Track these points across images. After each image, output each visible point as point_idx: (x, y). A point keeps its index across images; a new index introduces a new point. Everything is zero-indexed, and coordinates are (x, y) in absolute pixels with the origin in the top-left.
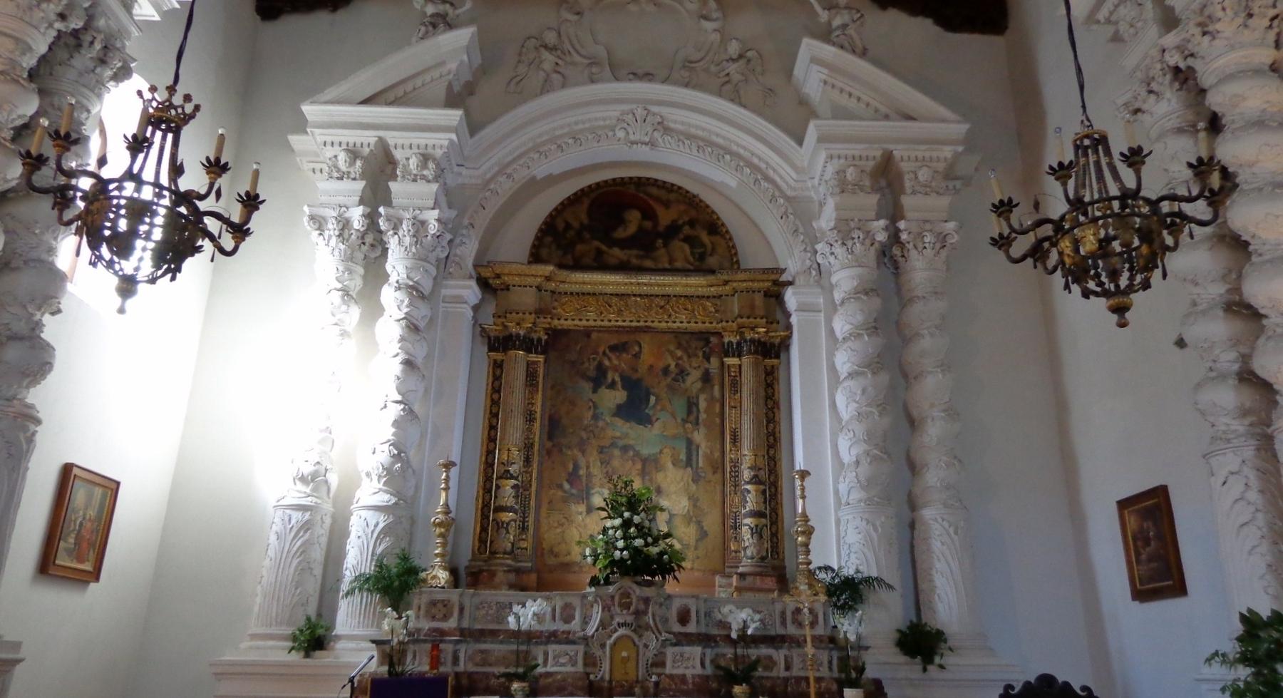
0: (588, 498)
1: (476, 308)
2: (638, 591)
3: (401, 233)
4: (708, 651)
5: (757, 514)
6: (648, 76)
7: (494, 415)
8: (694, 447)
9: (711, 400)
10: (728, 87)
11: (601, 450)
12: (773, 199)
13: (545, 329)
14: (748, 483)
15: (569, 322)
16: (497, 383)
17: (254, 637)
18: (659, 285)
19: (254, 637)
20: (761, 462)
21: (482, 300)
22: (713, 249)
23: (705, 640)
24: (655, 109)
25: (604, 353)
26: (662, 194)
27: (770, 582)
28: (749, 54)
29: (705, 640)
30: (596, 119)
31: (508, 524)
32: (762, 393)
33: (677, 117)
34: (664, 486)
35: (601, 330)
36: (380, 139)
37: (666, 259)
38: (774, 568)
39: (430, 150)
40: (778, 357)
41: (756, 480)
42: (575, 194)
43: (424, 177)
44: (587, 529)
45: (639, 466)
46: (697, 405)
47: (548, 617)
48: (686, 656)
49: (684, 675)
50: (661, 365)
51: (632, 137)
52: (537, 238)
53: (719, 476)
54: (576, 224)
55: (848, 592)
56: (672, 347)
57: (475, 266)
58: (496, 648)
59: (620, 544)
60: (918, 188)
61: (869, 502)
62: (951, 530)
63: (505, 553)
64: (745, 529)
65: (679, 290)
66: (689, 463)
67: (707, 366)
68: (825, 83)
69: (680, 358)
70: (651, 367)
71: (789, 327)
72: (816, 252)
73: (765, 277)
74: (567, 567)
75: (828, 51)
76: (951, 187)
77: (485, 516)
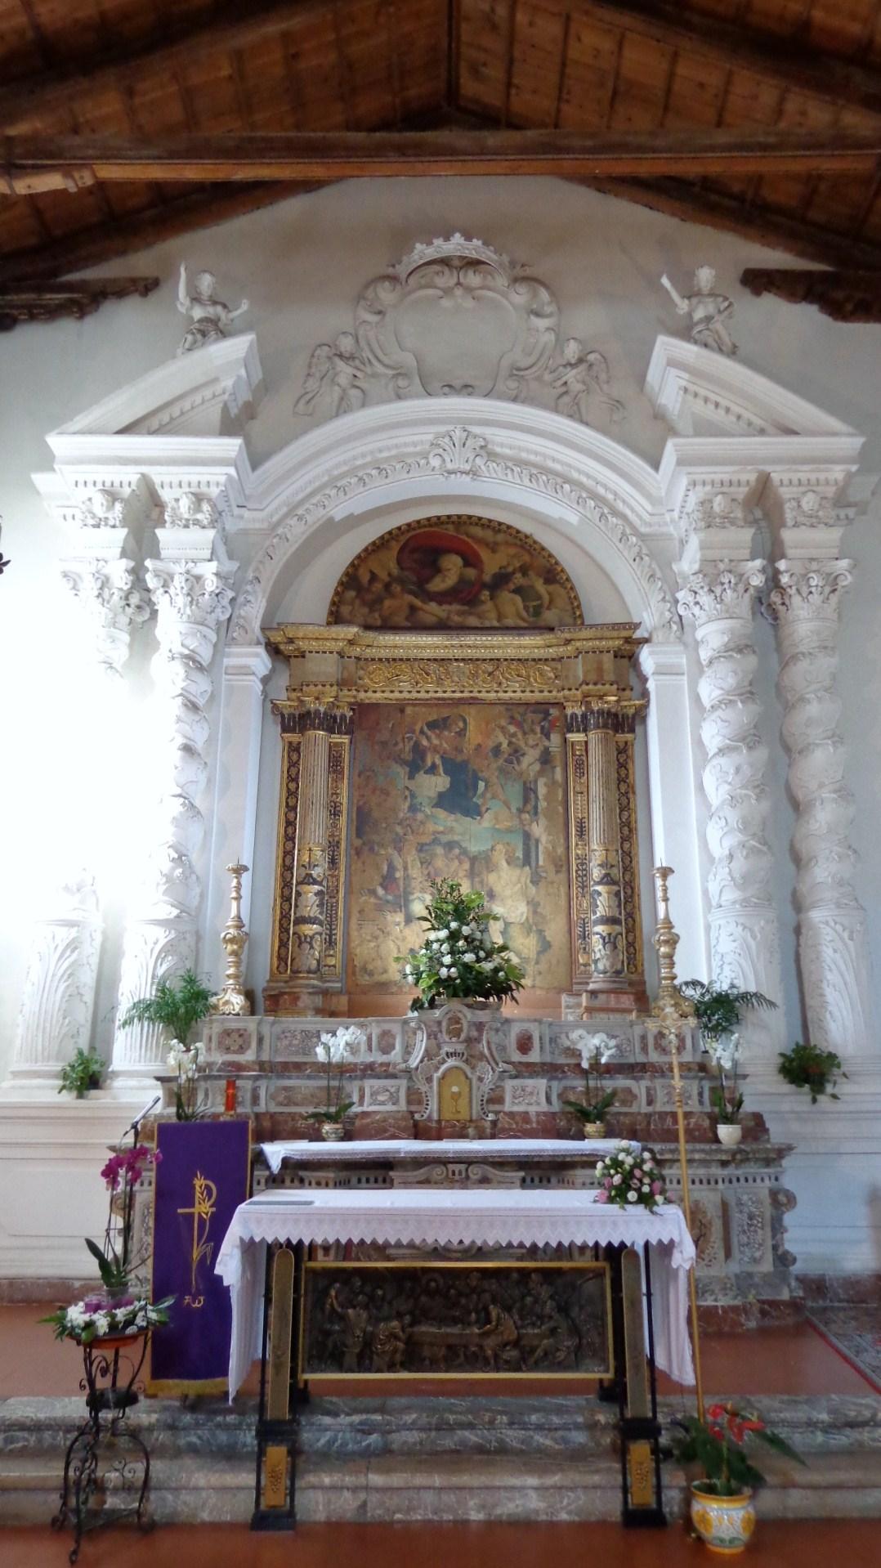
0: (406, 906)
1: (265, 681)
2: (468, 1016)
3: (172, 591)
4: (555, 1084)
5: (611, 921)
6: (467, 389)
7: (291, 808)
8: (532, 842)
9: (552, 784)
10: (566, 399)
11: (421, 848)
12: (623, 538)
13: (350, 704)
14: (599, 883)
15: (379, 695)
16: (293, 771)
17: (16, 1074)
18: (486, 647)
19: (16, 1074)
20: (614, 858)
21: (273, 670)
22: (551, 602)
23: (550, 1070)
24: (476, 430)
25: (422, 732)
26: (488, 535)
27: (627, 1001)
28: (591, 357)
29: (550, 1070)
30: (406, 445)
31: (312, 938)
33: (501, 439)
34: (497, 889)
35: (416, 703)
36: (143, 475)
37: (493, 615)
38: (631, 984)
39: (204, 489)
40: (632, 730)
41: (608, 880)
42: (382, 537)
43: (197, 522)
44: (405, 943)
45: (467, 866)
46: (535, 792)
47: (363, 1047)
48: (529, 1090)
49: (527, 1113)
50: (491, 744)
51: (450, 466)
52: (337, 593)
53: (563, 876)
54: (383, 575)
55: (721, 1010)
56: (503, 722)
57: (263, 629)
58: (304, 1085)
59: (447, 960)
60: (801, 519)
61: (745, 903)
62: (846, 935)
63: (309, 972)
64: (595, 938)
65: (511, 653)
66: (527, 861)
67: (547, 743)
68: (686, 390)
69: (514, 735)
70: (479, 745)
71: (645, 694)
72: (677, 601)
73: (615, 634)
74: (384, 987)
75: (688, 351)
76: (842, 516)
77: (284, 930)
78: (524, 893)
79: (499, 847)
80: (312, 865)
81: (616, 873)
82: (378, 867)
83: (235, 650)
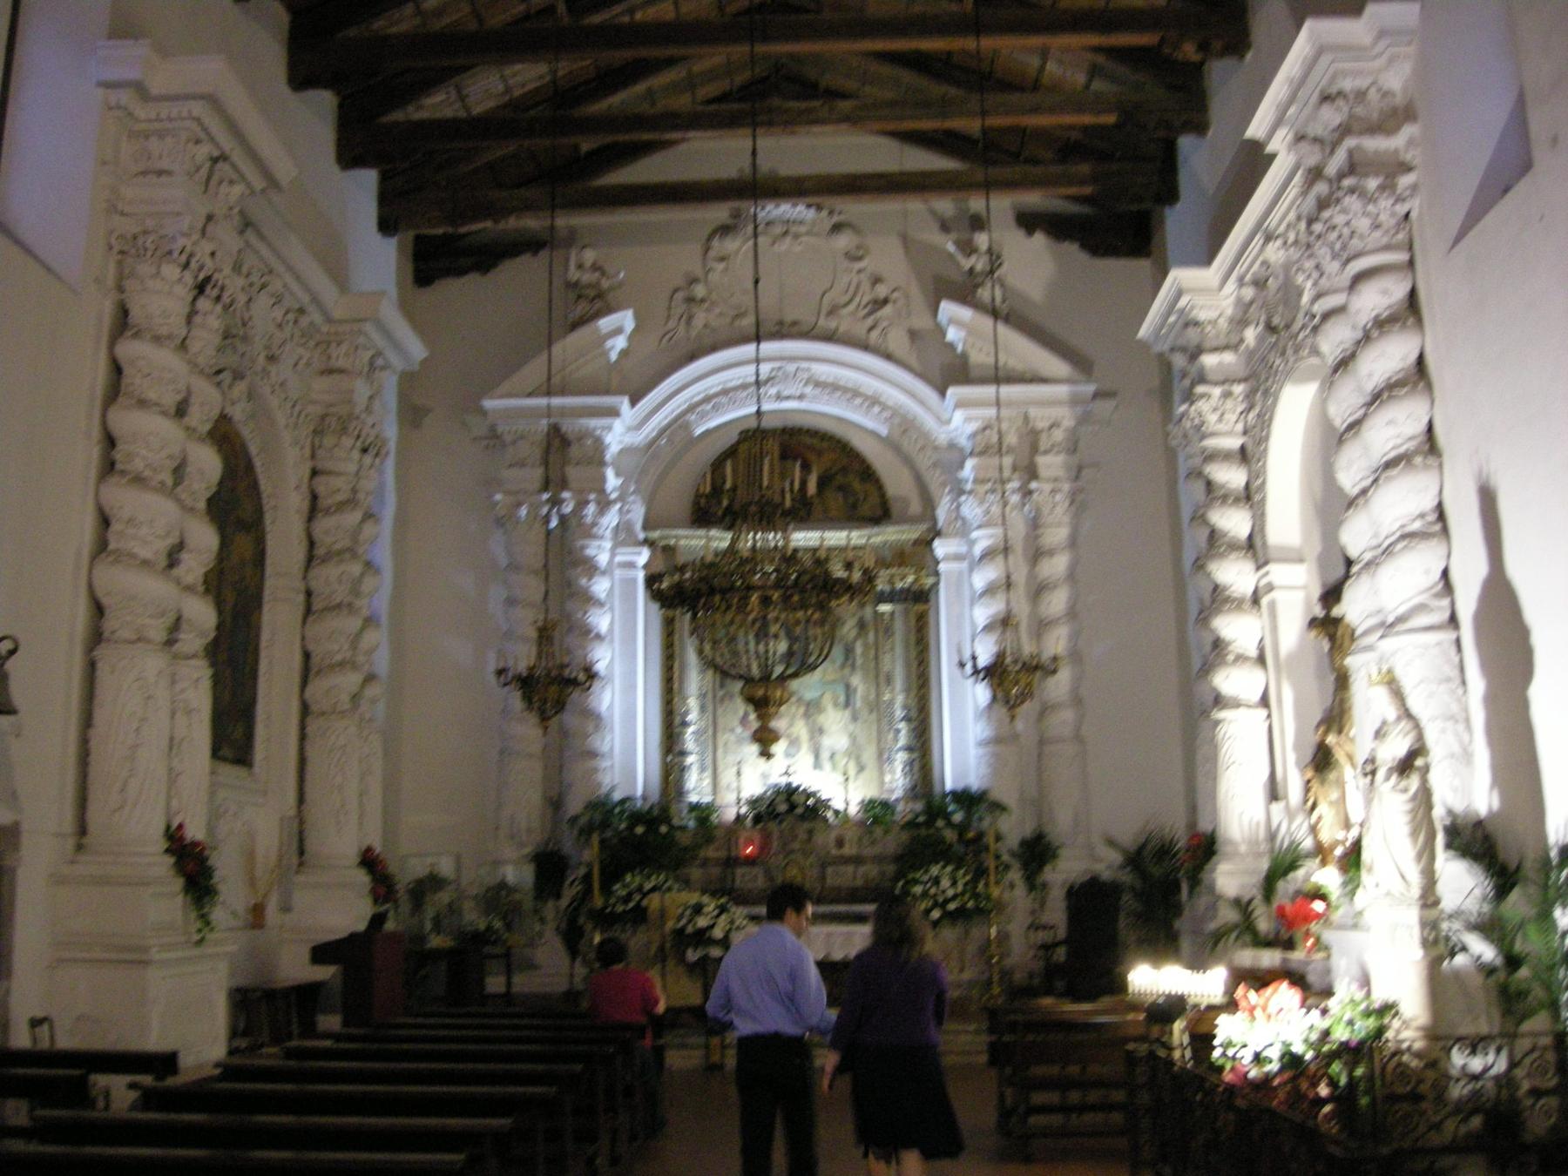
5: (909, 749)
9: (866, 645)
20: (913, 703)
34: (826, 727)
40: (927, 601)
45: (802, 710)
53: (874, 716)
66: (847, 704)
71: (937, 574)
80: (687, 713)
81: (914, 714)
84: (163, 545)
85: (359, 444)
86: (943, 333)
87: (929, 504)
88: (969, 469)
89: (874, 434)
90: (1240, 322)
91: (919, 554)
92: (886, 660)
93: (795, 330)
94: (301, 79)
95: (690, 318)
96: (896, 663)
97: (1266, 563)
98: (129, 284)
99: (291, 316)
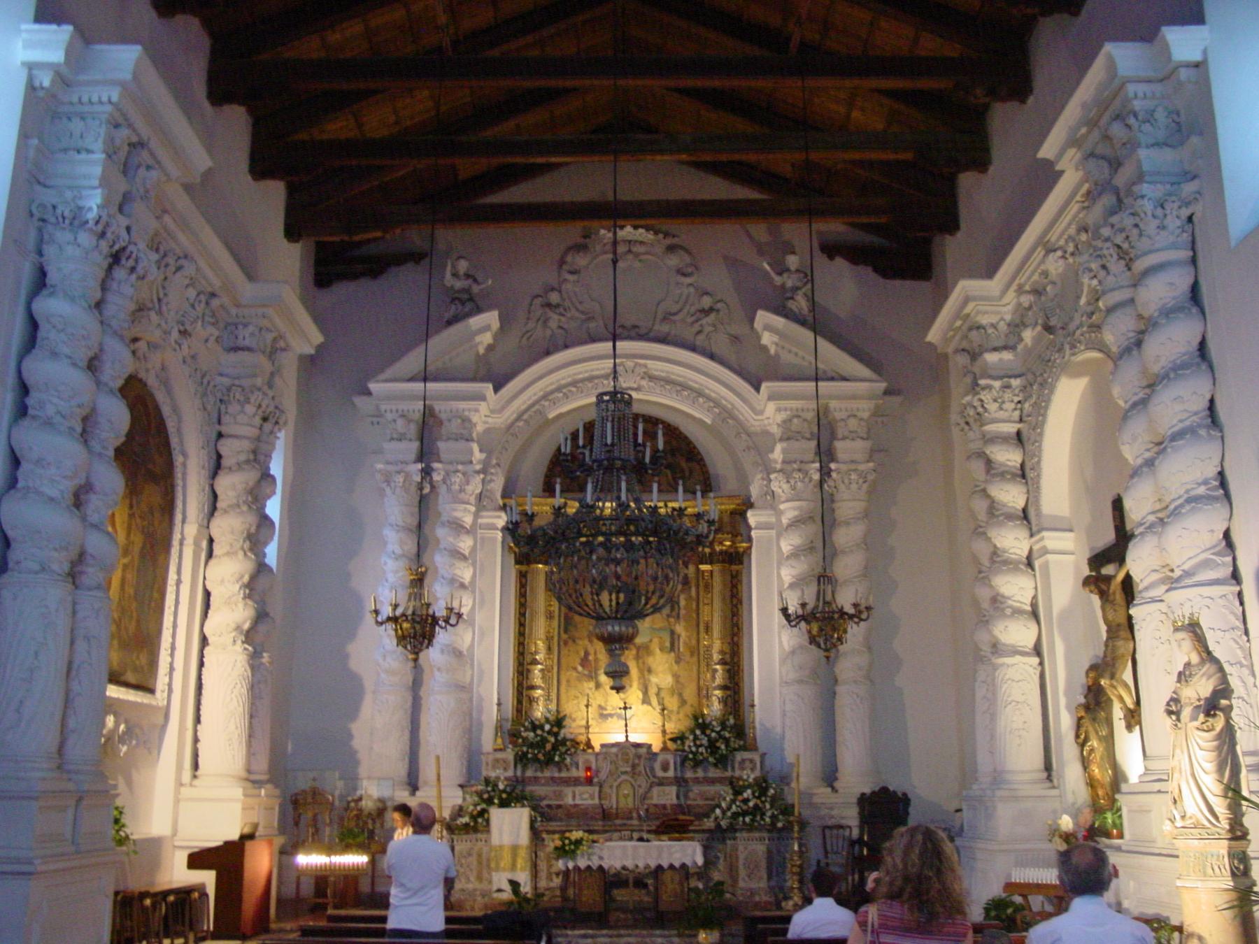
5: (724, 688)
9: (689, 598)
20: (727, 649)
32: (728, 594)
33: (656, 367)
34: (654, 666)
40: (741, 563)
46: (678, 603)
53: (695, 659)
57: (503, 497)
71: (750, 539)
78: (670, 669)
79: (656, 640)
80: (536, 653)
81: (728, 657)
82: (578, 652)
83: (484, 514)
84: (69, 486)
85: (260, 412)
86: (759, 338)
87: (744, 480)
88: (777, 454)
89: (701, 422)
90: (1016, 326)
91: (736, 521)
92: (705, 610)
93: (633, 333)
94: (220, 94)
95: (545, 322)
96: (715, 613)
97: (1039, 531)
98: (50, 251)
99: (203, 298)
